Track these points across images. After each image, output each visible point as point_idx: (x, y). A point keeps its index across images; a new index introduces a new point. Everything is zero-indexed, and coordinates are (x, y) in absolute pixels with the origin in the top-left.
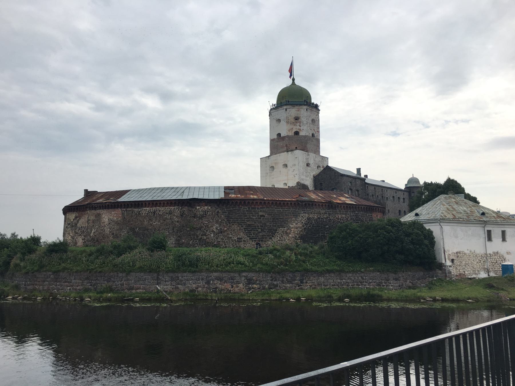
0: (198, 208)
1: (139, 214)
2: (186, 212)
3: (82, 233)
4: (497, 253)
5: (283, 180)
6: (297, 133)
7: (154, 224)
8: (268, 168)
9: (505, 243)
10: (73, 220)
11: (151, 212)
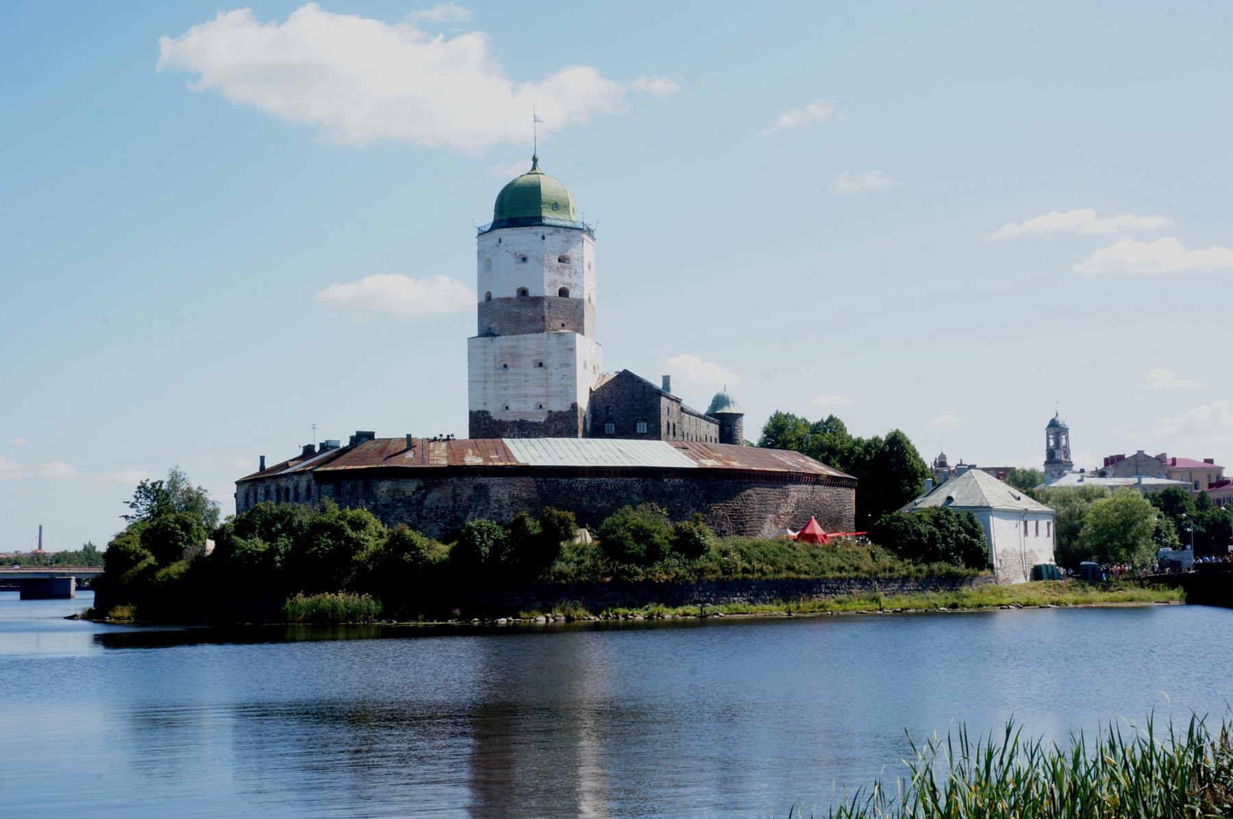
0: (666, 480)
1: (571, 488)
2: (650, 488)
3: (438, 519)
4: (1032, 551)
5: (536, 396)
6: (563, 292)
7: (599, 505)
8: (491, 364)
9: (1038, 538)
10: (410, 494)
11: (593, 486)
